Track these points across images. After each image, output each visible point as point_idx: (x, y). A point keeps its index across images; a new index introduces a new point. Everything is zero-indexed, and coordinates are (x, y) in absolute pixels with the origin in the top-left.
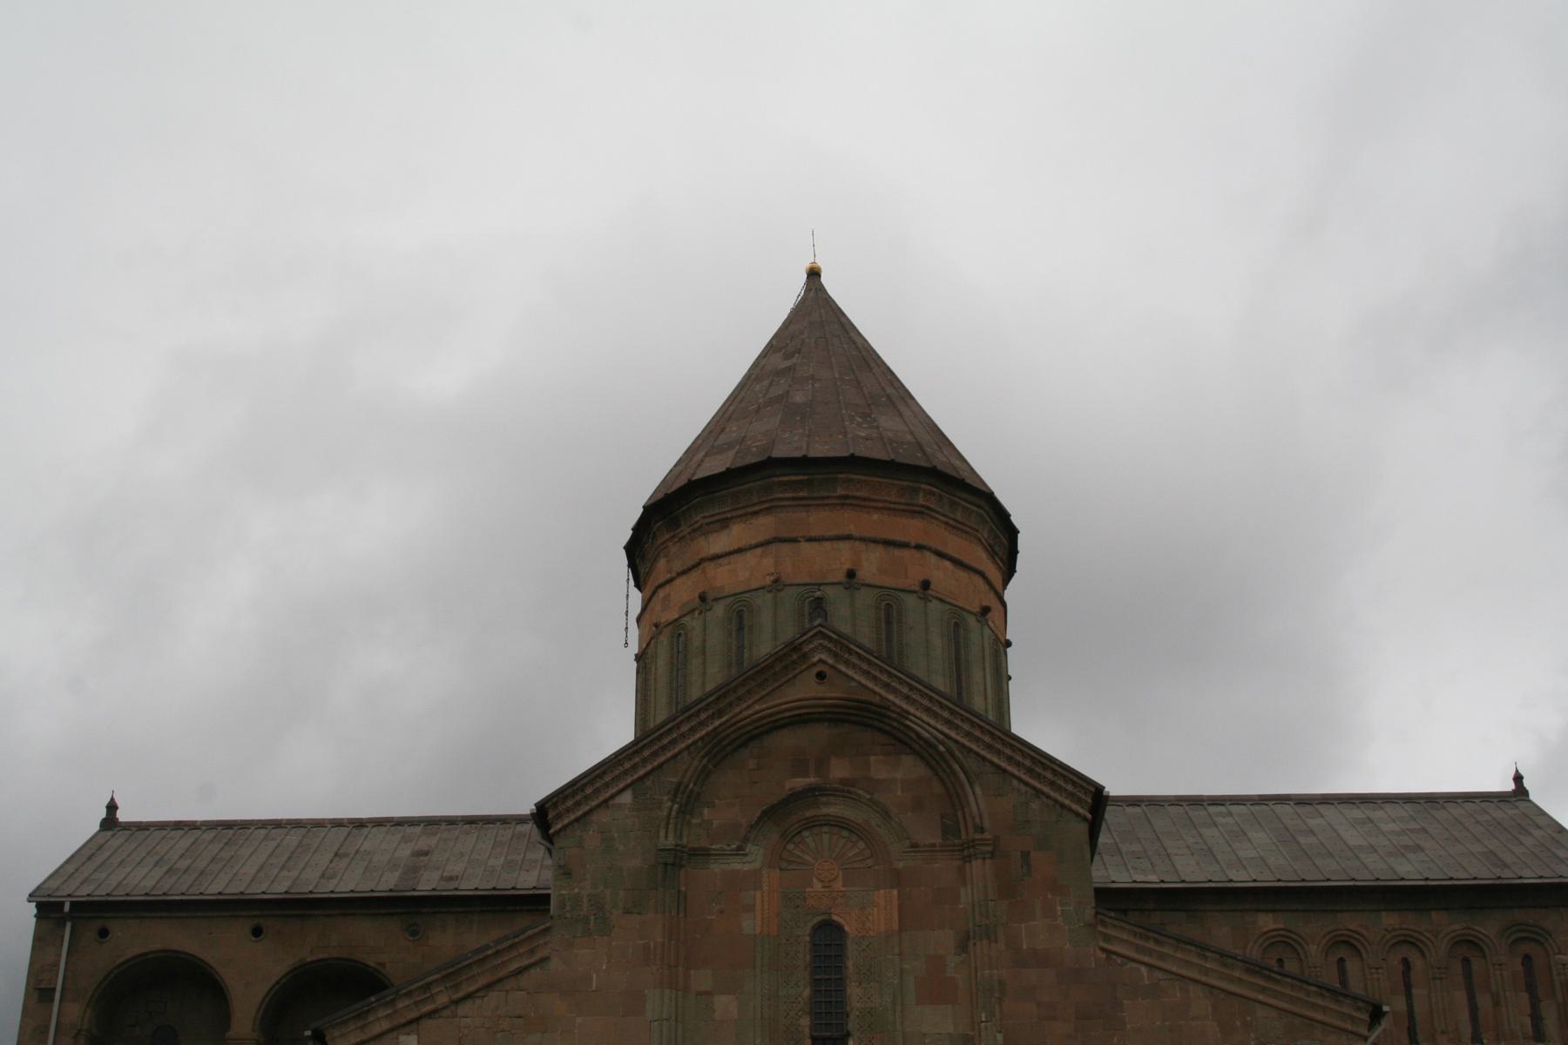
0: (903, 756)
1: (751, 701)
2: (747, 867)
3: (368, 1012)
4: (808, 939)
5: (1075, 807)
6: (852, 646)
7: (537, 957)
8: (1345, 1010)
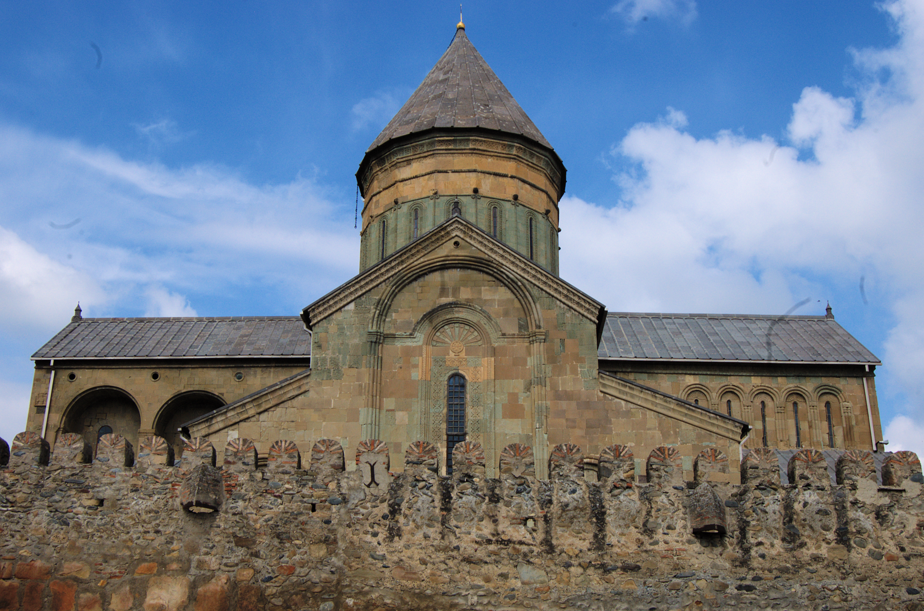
0: (499, 288)
1: (419, 257)
2: (414, 344)
3: (212, 418)
4: (446, 383)
5: (589, 316)
6: (473, 228)
7: (302, 390)
8: (729, 427)
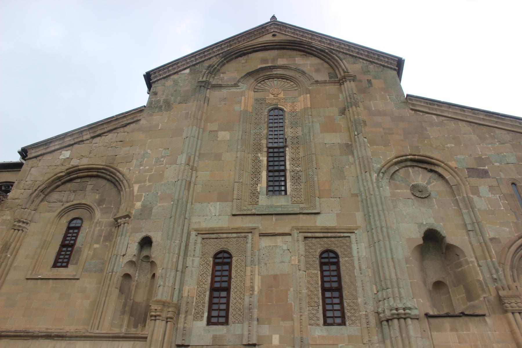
2: (238, 90)
4: (267, 113)
7: (135, 119)
